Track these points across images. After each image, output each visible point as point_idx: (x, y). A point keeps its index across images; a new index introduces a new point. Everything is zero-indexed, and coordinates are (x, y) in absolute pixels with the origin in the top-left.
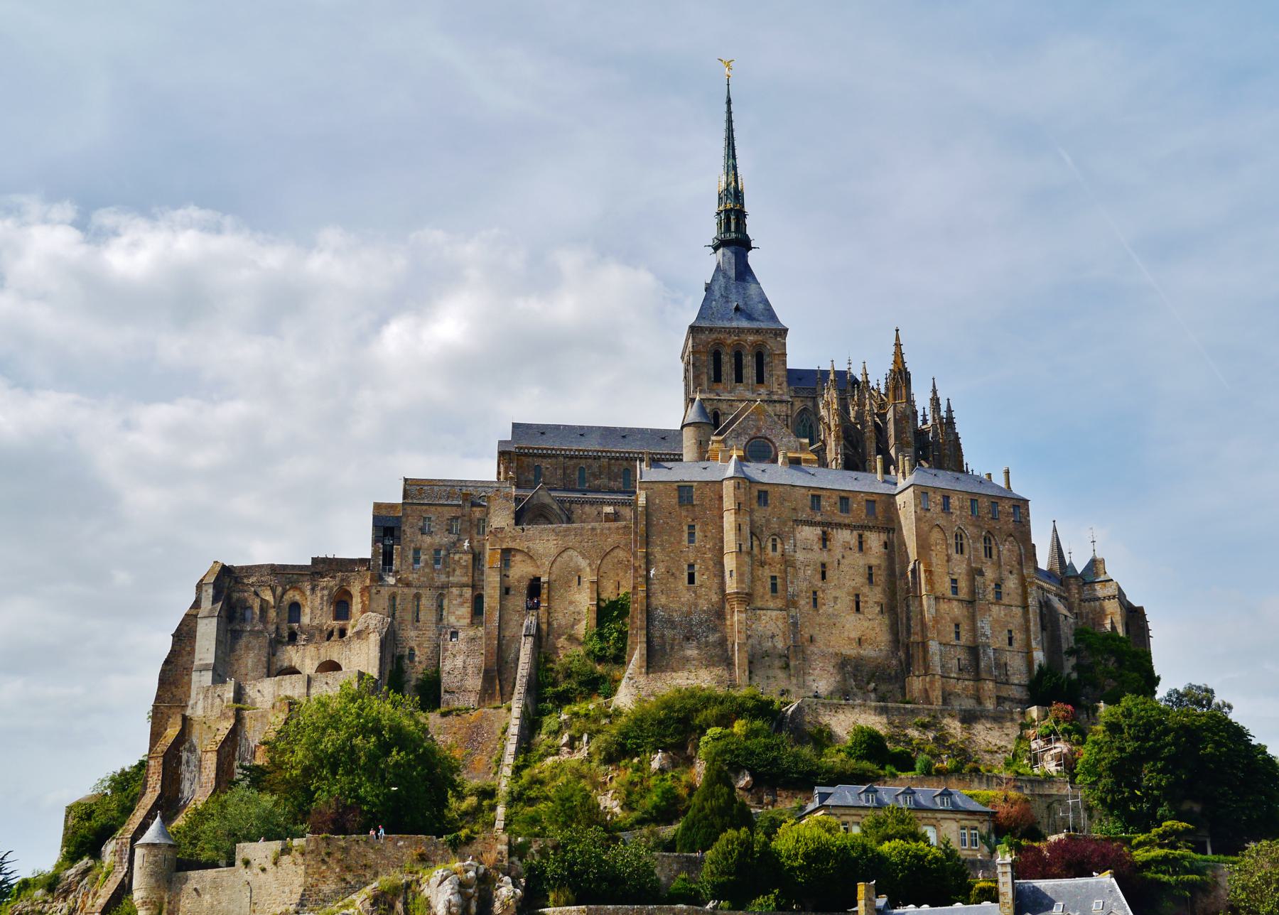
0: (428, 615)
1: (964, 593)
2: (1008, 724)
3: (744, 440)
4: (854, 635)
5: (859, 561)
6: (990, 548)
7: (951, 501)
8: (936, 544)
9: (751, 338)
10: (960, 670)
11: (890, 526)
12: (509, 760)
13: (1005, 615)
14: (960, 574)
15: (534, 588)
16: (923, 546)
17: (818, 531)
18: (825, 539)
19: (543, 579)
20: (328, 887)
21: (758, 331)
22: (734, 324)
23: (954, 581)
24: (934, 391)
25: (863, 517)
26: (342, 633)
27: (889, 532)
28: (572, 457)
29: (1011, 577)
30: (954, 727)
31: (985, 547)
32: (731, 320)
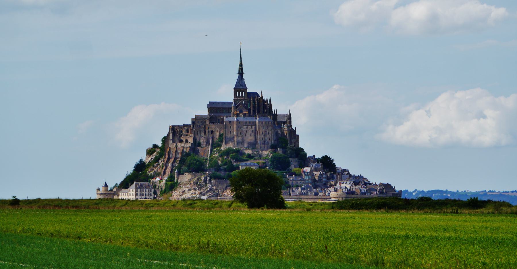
0: (199, 134)
2: (267, 151)
3: (239, 110)
4: (250, 139)
11: (255, 125)
12: (209, 155)
15: (212, 131)
16: (259, 128)
18: (247, 127)
20: (193, 177)
21: (243, 89)
22: (240, 88)
23: (263, 133)
26: (188, 135)
30: (260, 152)
32: (240, 87)
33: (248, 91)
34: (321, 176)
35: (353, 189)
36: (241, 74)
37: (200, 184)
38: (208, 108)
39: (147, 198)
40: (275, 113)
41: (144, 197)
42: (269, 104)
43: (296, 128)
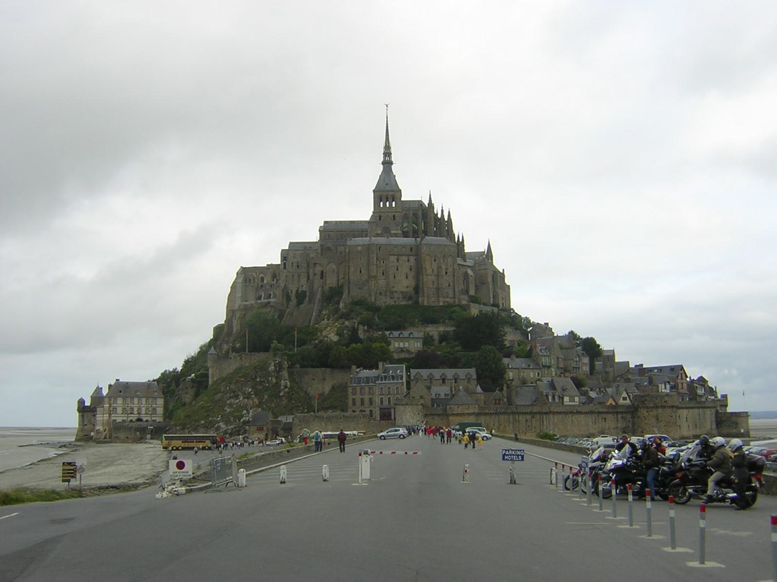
4: (406, 286)
5: (407, 264)
9: (391, 193)
10: (434, 295)
17: (396, 257)
18: (398, 260)
19: (324, 271)
21: (392, 191)
22: (386, 189)
23: (433, 270)
24: (442, 208)
28: (338, 231)
33: (403, 199)
34: (578, 359)
35: (682, 384)
36: (387, 164)
37: (261, 381)
38: (320, 231)
39: (145, 419)
40: (461, 240)
41: (134, 417)
42: (446, 222)
43: (503, 270)
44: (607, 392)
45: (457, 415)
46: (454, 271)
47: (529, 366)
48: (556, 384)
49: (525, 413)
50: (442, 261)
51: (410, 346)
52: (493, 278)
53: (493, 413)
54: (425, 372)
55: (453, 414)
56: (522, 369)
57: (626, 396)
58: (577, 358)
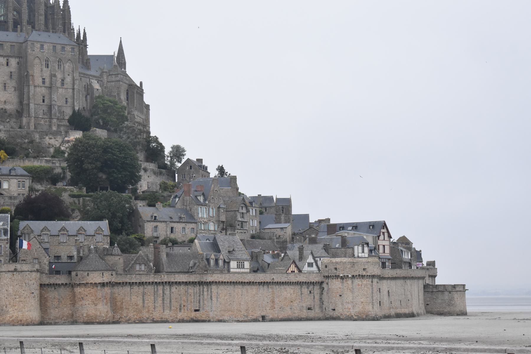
1: (47, 84)
4: (3, 100)
5: (7, 70)
6: (61, 65)
7: (44, 47)
8: (37, 64)
13: (65, 92)
14: (46, 76)
23: (43, 79)
25: (9, 52)
27: (20, 58)
29: (68, 77)
30: (37, 137)
31: (58, 65)
34: (244, 211)
40: (82, 38)
42: (63, 11)
43: (141, 83)
44: (288, 256)
45: (86, 285)
46: (74, 80)
47: (180, 218)
48: (220, 244)
49: (180, 282)
50: (57, 67)
51: (11, 188)
52: (127, 93)
53: (136, 283)
54: (37, 225)
55: (80, 285)
56: (171, 222)
57: (312, 261)
58: (244, 209)
